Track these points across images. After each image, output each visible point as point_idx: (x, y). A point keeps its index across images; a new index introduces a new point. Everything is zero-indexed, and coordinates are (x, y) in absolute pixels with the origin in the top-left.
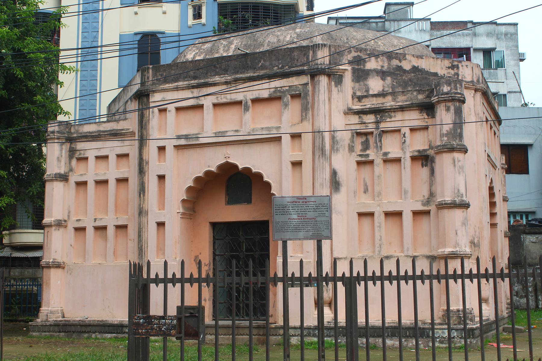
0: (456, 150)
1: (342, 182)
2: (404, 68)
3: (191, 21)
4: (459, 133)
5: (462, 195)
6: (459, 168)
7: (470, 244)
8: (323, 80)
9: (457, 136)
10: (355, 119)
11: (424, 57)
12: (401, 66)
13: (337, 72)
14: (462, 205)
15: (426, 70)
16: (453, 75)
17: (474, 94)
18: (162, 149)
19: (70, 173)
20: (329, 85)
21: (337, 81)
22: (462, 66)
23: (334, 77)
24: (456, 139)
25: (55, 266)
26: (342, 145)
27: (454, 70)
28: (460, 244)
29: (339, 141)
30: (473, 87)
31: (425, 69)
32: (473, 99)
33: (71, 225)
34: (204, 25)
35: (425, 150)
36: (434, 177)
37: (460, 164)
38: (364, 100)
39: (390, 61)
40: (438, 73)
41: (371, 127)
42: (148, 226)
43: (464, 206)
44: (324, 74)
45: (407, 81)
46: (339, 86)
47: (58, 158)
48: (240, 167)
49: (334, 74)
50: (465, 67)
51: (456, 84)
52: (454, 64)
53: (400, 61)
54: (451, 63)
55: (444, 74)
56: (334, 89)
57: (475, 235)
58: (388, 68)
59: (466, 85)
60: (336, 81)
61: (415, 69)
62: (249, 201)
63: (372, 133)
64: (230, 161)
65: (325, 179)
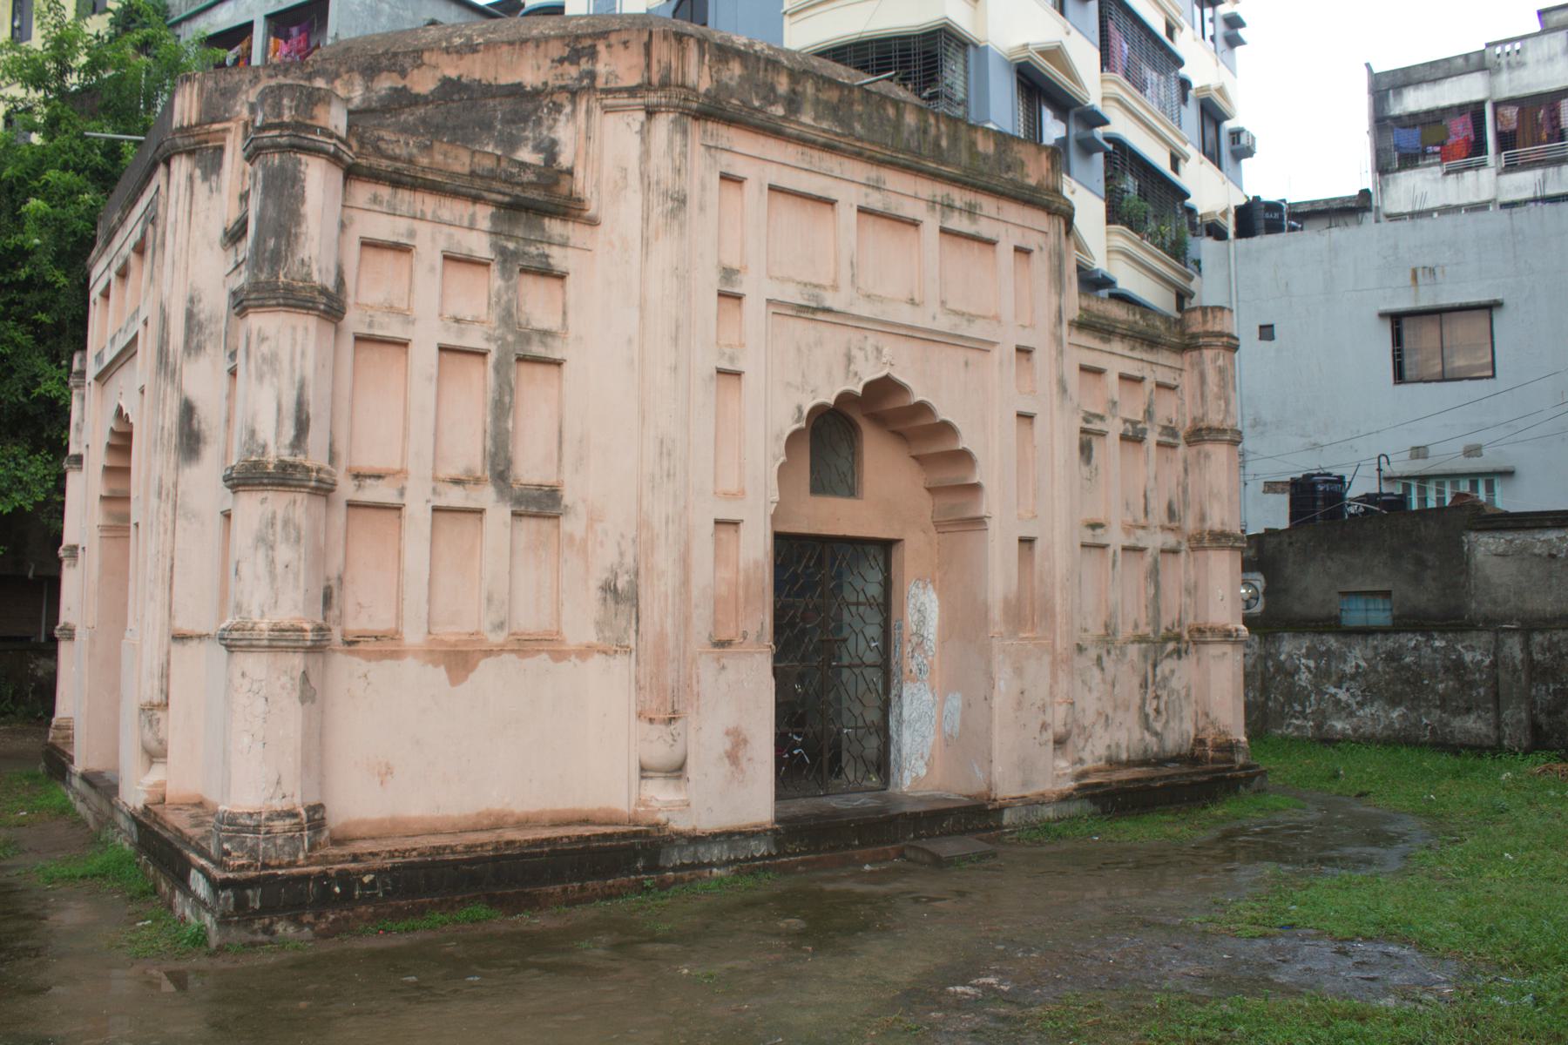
0: (250, 307)
1: (207, 433)
2: (413, 92)
4: (273, 251)
5: (264, 447)
6: (260, 361)
7: (599, 594)
8: (181, 167)
9: (264, 261)
11: (482, 47)
12: (405, 87)
13: (207, 142)
14: (250, 482)
15: (484, 82)
16: (576, 79)
17: (642, 125)
20: (191, 178)
21: (209, 164)
22: (609, 46)
23: (201, 155)
24: (261, 270)
26: (212, 334)
27: (578, 64)
28: (245, 606)
29: (205, 323)
30: (631, 101)
31: (480, 81)
32: (637, 139)
37: (265, 348)
39: (372, 81)
40: (525, 84)
43: (257, 482)
44: (180, 153)
45: (414, 124)
46: (214, 178)
47: (77, 425)
49: (200, 148)
50: (619, 49)
51: (281, 99)
52: (580, 46)
53: (403, 74)
54: (568, 45)
55: (545, 84)
56: (201, 188)
57: (621, 564)
58: (364, 101)
59: (605, 102)
60: (206, 167)
61: (450, 88)
65: (163, 428)
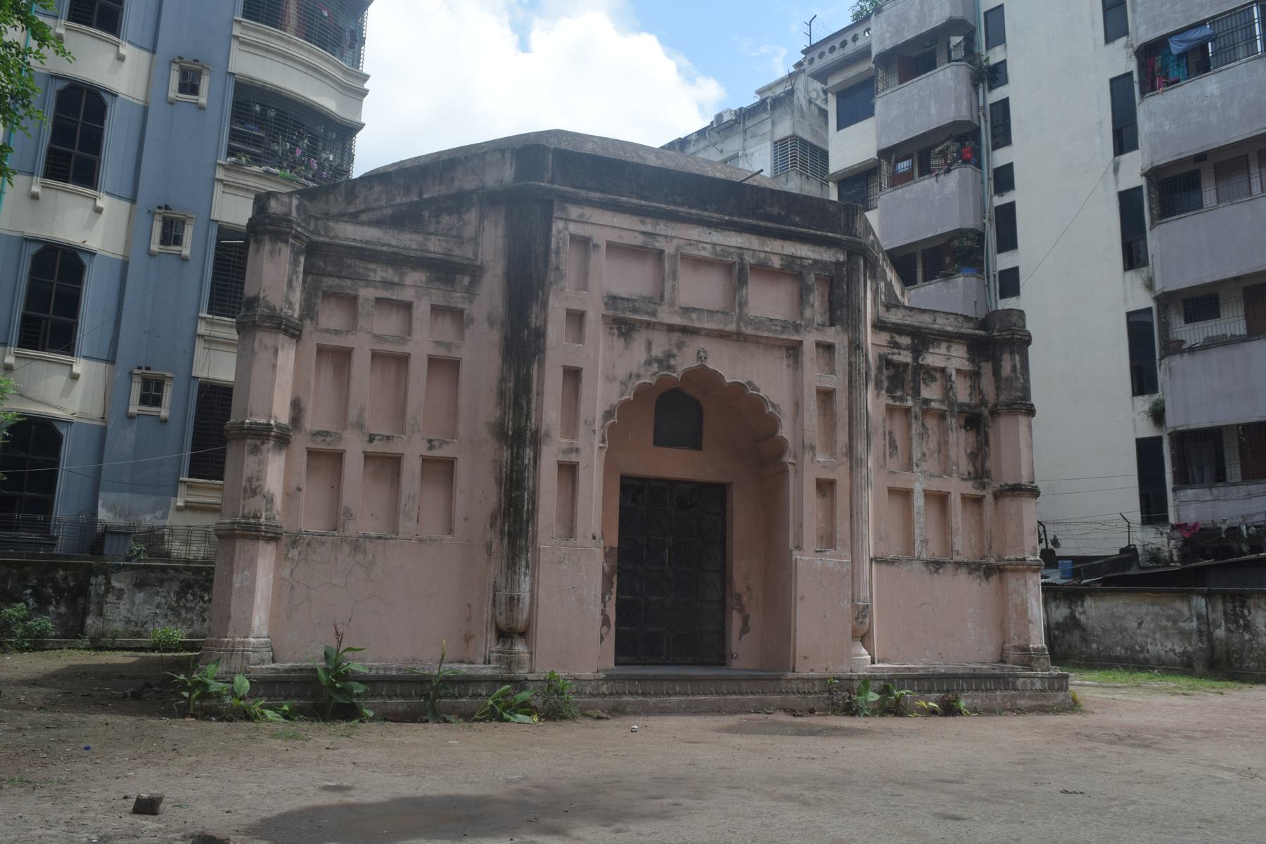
3: (173, 93)
10: (884, 338)
18: (576, 318)
19: (307, 322)
25: (269, 535)
33: (300, 443)
34: (201, 108)
35: (977, 406)
36: (989, 447)
38: (893, 310)
41: (905, 357)
42: (535, 468)
48: (728, 380)
62: (696, 444)
63: (906, 365)
64: (711, 365)
